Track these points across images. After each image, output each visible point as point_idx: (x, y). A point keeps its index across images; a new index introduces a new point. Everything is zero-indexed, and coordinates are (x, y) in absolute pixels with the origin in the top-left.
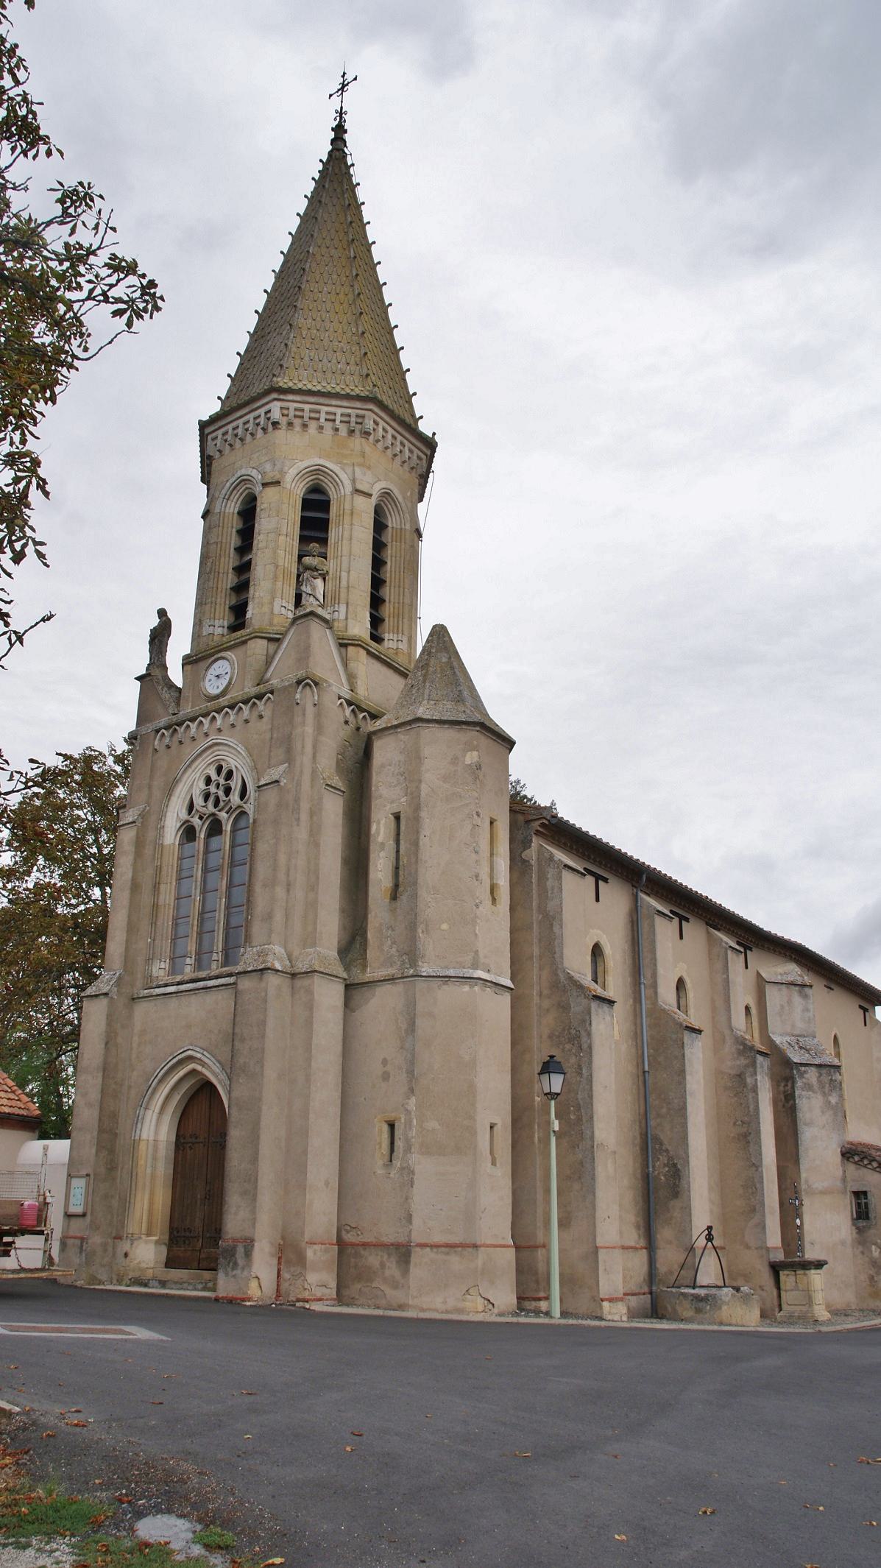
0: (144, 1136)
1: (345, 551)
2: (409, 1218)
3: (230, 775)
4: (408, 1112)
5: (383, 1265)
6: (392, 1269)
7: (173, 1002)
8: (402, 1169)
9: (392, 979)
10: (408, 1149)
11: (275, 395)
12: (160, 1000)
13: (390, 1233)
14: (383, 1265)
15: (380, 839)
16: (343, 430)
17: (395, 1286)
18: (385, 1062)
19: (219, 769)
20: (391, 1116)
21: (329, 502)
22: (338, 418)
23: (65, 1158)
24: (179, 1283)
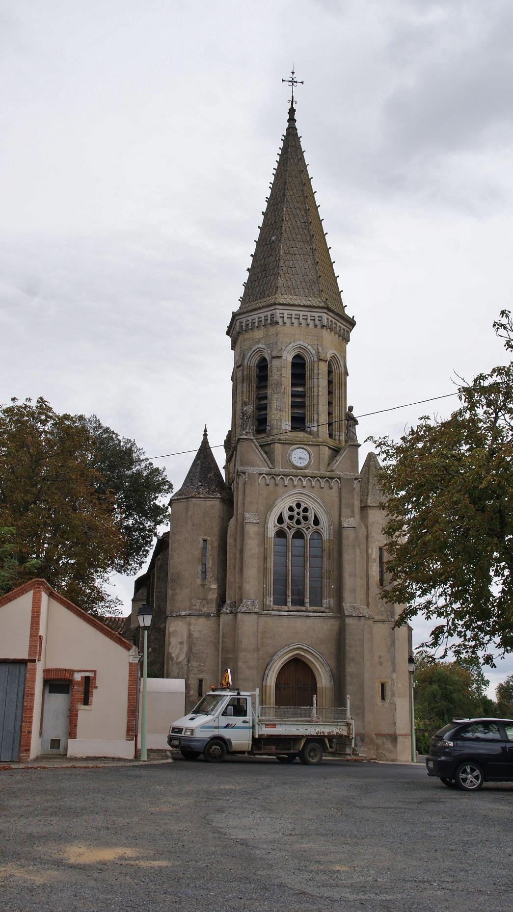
0: (268, 684)
1: (315, 394)
2: (395, 723)
3: (306, 510)
4: (393, 680)
5: (383, 743)
6: (388, 745)
7: (285, 620)
8: (390, 703)
9: (383, 621)
10: (393, 695)
11: (326, 311)
12: (304, 619)
13: (386, 730)
14: (383, 743)
15: (374, 557)
16: (311, 326)
17: (390, 752)
18: (380, 657)
19: (298, 506)
20: (384, 680)
21: (304, 364)
22: (309, 318)
23: (183, 689)
24: (155, 759)
